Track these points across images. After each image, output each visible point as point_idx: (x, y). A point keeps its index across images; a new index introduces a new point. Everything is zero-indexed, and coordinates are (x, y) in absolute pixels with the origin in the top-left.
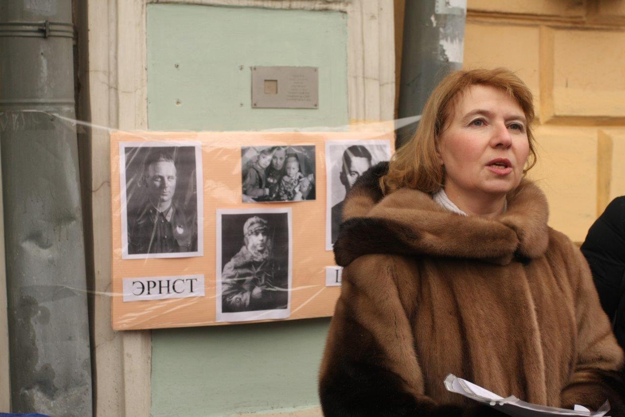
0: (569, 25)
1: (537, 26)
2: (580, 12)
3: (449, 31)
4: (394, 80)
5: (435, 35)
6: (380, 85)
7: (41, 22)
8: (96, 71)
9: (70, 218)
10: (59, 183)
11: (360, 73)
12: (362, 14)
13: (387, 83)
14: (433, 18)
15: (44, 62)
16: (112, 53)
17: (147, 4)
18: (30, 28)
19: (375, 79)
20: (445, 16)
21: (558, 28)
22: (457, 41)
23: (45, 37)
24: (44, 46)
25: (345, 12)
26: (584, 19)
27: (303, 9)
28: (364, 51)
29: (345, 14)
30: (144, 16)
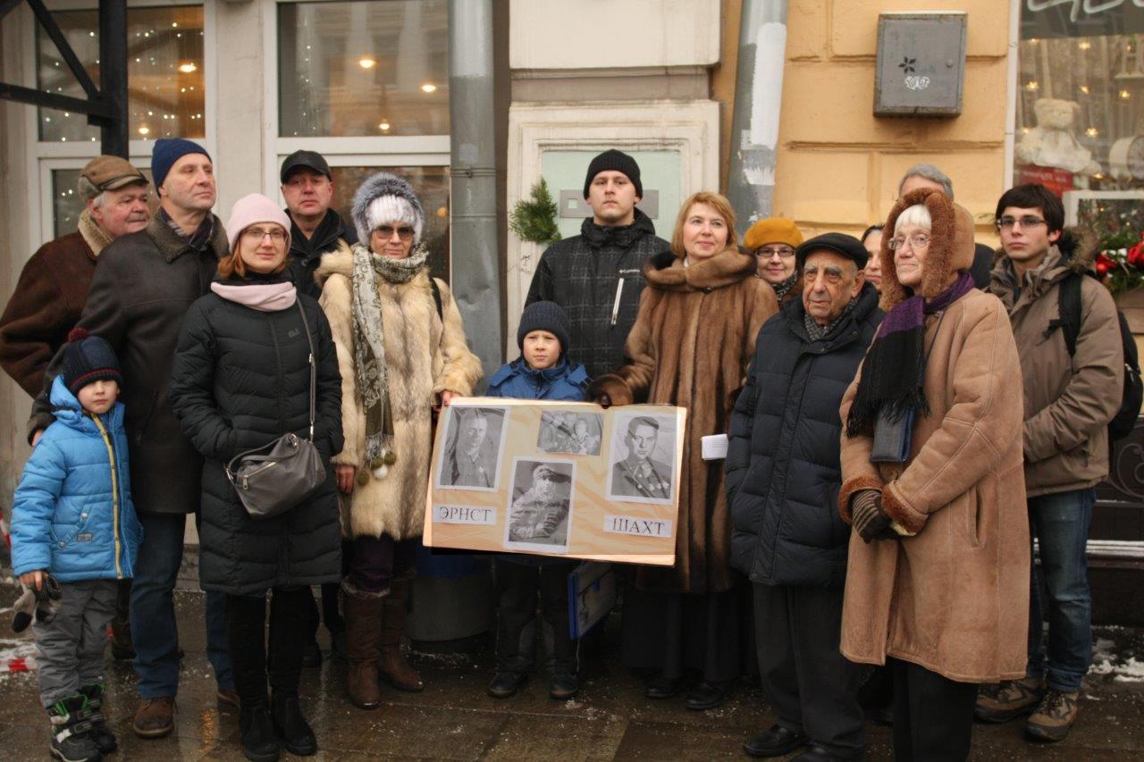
0: (901, 150)
1: (869, 152)
2: (909, 140)
3: (751, 161)
5: (740, 165)
7: (469, 167)
9: (486, 287)
10: (478, 264)
14: (739, 153)
15: (469, 191)
18: (462, 172)
20: (748, 151)
21: (888, 153)
22: (759, 169)
23: (470, 177)
24: (469, 182)
26: (914, 145)
27: (648, 150)
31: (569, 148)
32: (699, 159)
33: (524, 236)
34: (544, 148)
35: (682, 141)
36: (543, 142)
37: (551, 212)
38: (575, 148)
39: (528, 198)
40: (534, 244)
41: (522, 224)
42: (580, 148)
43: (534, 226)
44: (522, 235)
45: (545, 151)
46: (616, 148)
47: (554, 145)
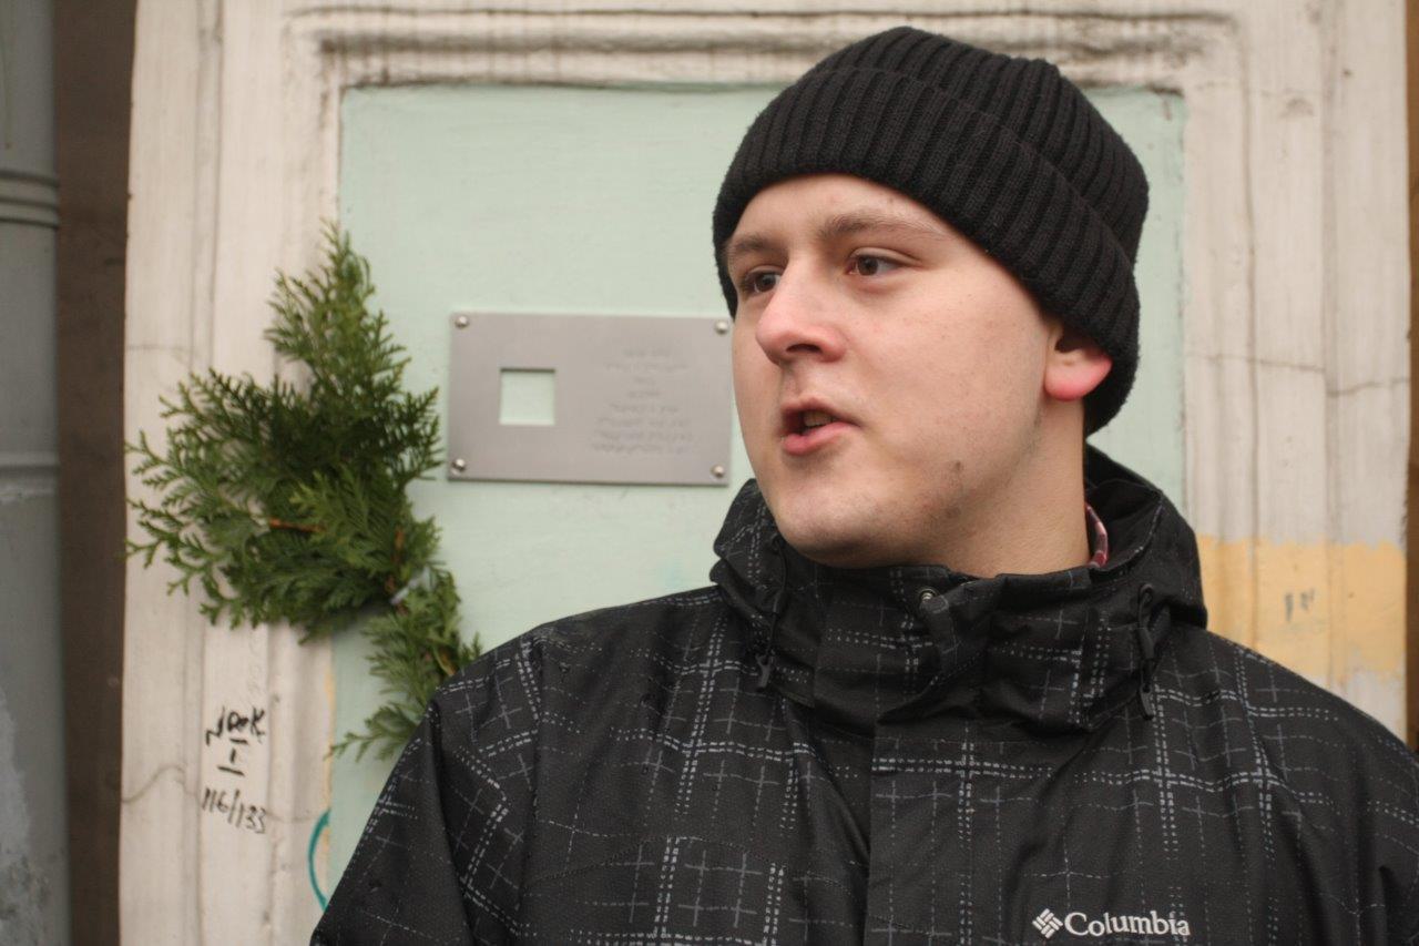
4: (1405, 370)
6: (1332, 393)
8: (147, 347)
11: (1237, 346)
12: (1246, 92)
13: (1371, 384)
16: (202, 280)
17: (344, 90)
19: (1304, 368)
25: (1175, 92)
28: (1252, 252)
29: (1173, 100)
30: (331, 135)
31: (503, 66)
32: (1303, 135)
33: (227, 590)
34: (356, 67)
35: (1194, 29)
36: (348, 25)
37: (397, 447)
38: (541, 65)
39: (250, 358)
40: (287, 639)
41: (215, 517)
42: (571, 66)
43: (291, 529)
44: (213, 592)
45: (363, 84)
46: (918, 25)
47: (412, 45)
